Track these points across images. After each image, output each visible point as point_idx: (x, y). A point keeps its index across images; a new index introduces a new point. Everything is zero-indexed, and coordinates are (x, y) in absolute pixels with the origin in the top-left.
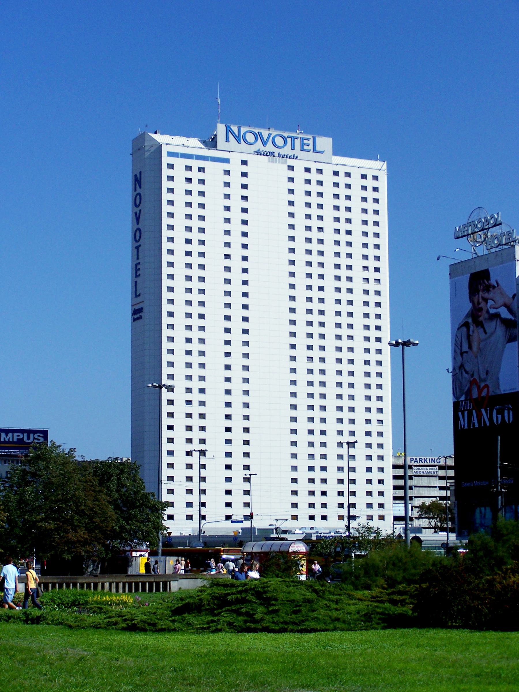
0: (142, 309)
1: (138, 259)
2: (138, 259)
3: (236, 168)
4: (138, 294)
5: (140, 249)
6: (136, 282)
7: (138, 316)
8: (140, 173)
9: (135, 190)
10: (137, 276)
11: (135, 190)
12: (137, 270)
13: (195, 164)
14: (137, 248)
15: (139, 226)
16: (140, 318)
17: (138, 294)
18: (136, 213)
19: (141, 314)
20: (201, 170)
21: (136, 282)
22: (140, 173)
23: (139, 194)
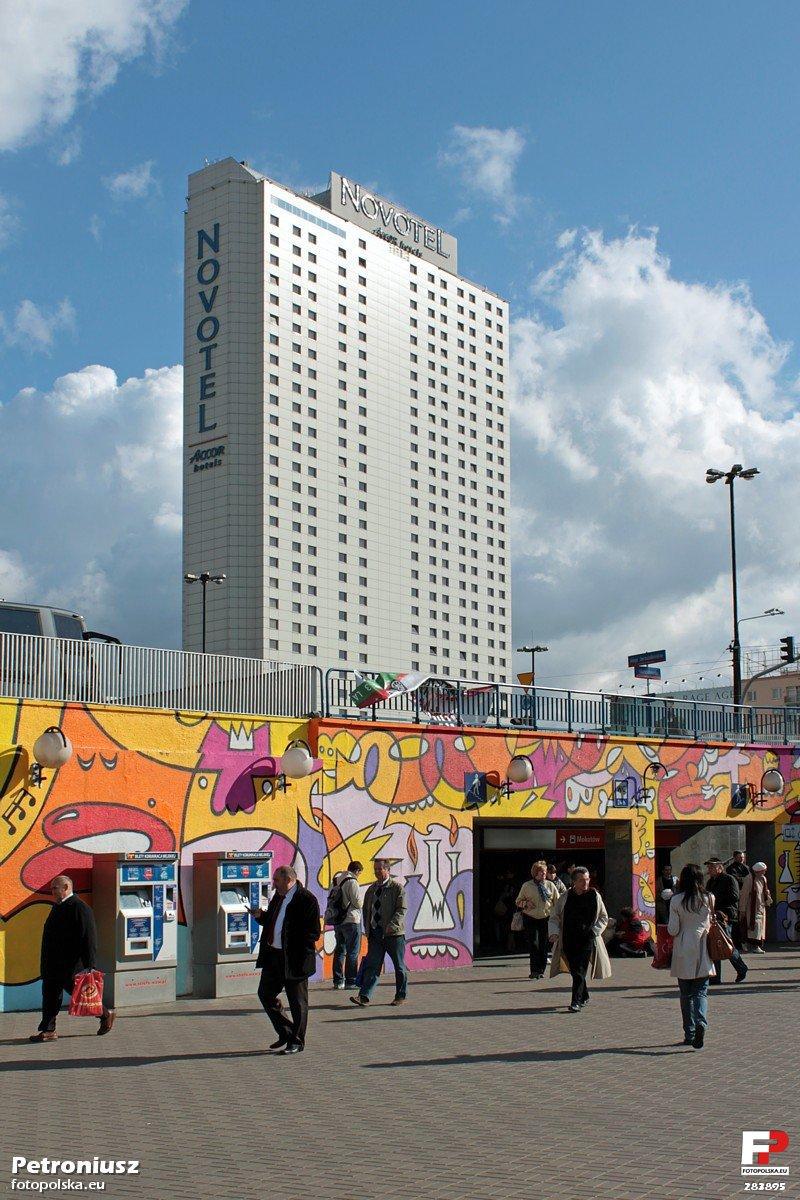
0: (220, 450)
1: (208, 367)
2: (208, 367)
3: (355, 252)
4: (208, 424)
5: (213, 352)
6: (202, 408)
7: (212, 460)
8: (217, 227)
9: (200, 256)
10: (204, 396)
11: (200, 256)
12: (204, 387)
13: (308, 228)
14: (207, 350)
15: (211, 314)
16: (220, 463)
17: (208, 424)
18: (202, 294)
19: (218, 458)
20: (313, 239)
21: (202, 408)
22: (217, 227)
23: (215, 263)
